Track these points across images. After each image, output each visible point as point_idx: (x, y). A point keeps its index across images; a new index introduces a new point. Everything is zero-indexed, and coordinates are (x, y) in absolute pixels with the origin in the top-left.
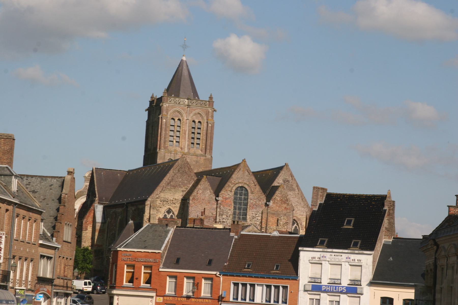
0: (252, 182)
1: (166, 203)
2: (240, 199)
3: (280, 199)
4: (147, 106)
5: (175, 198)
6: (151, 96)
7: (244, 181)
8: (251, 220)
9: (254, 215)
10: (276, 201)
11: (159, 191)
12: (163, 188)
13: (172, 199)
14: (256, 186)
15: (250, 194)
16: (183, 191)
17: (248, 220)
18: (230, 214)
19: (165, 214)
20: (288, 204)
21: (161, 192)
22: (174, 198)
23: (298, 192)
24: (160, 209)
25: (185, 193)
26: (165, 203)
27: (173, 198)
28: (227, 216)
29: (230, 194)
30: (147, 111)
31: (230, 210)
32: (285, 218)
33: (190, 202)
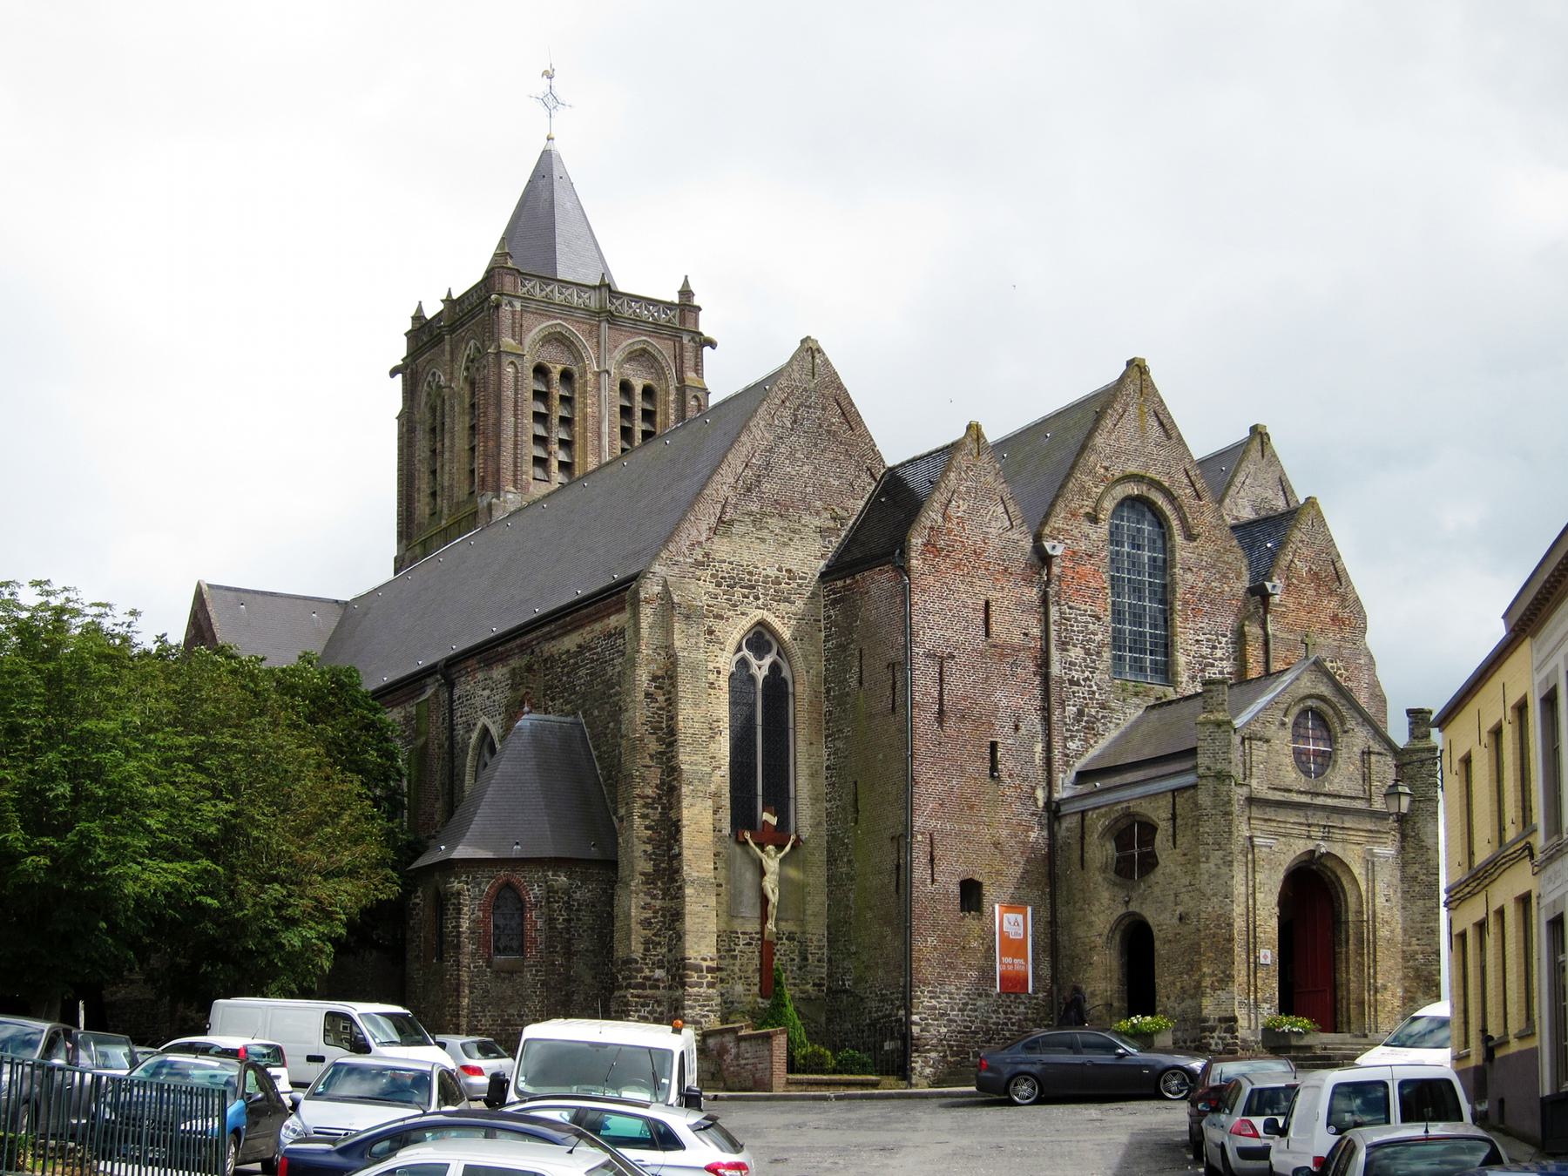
0: (1186, 481)
1: (746, 591)
2: (1135, 563)
3: (1311, 569)
4: (398, 351)
5: (789, 571)
6: (412, 313)
7: (1147, 466)
8: (1193, 678)
9: (1206, 651)
11: (704, 527)
12: (723, 512)
13: (773, 572)
14: (1200, 499)
15: (1179, 539)
16: (822, 532)
17: (1184, 678)
18: (1101, 645)
22: (785, 566)
24: (718, 626)
25: (836, 541)
27: (780, 570)
28: (1088, 652)
29: (1094, 537)
30: (399, 376)
31: (1099, 619)
33: (914, 562)
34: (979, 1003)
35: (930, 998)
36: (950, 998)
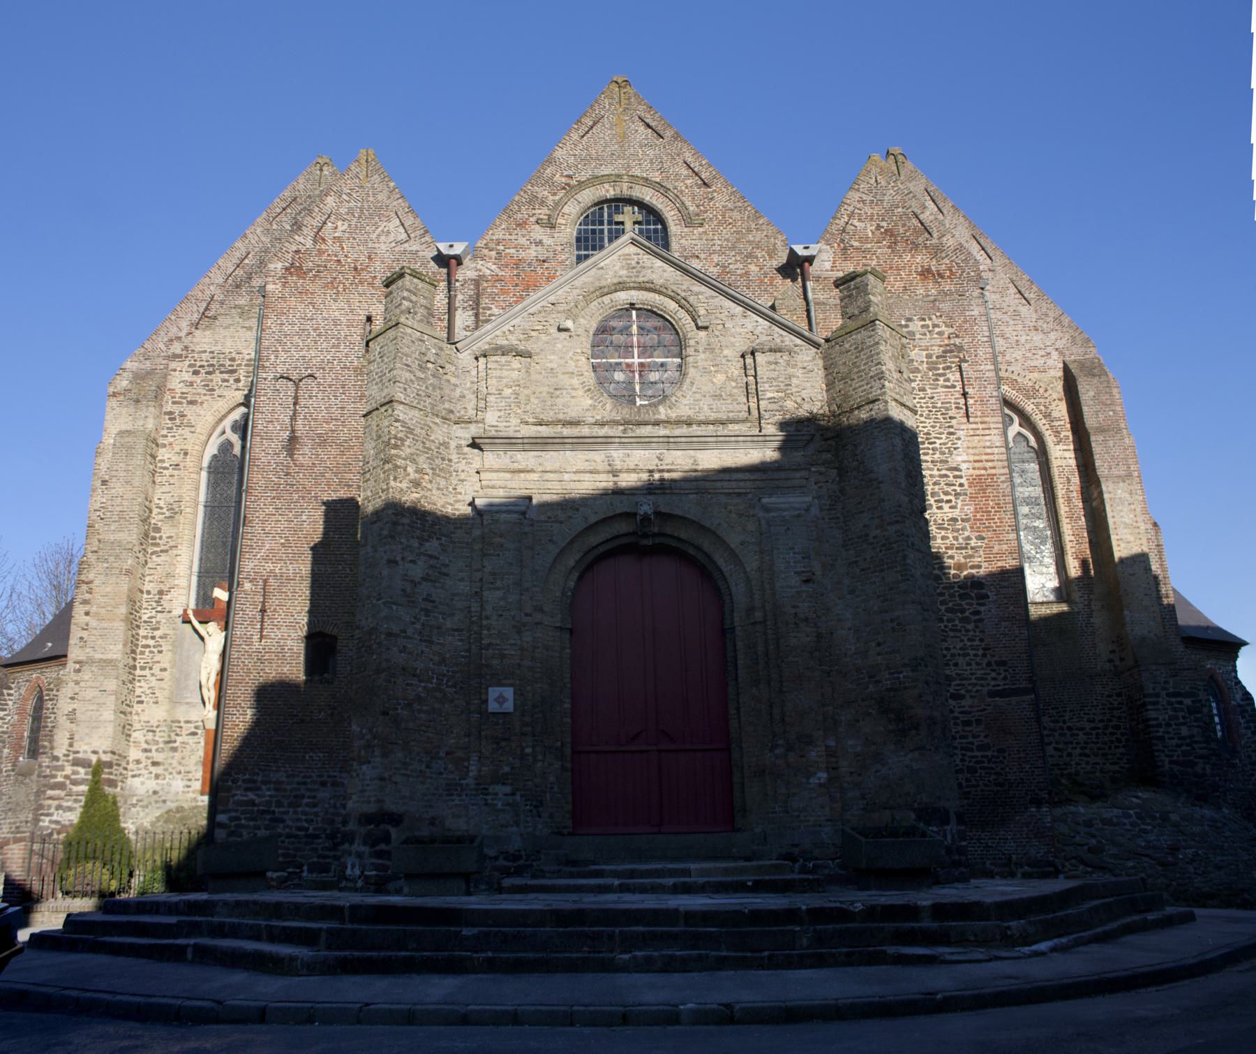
1: (226, 376)
3: (878, 227)
10: (856, 244)
11: (184, 325)
12: (207, 309)
19: (224, 437)
20: (937, 251)
21: (196, 326)
23: (988, 261)
24: (190, 411)
26: (217, 377)
32: (935, 326)
34: (321, 795)
35: (247, 789)
36: (276, 790)
